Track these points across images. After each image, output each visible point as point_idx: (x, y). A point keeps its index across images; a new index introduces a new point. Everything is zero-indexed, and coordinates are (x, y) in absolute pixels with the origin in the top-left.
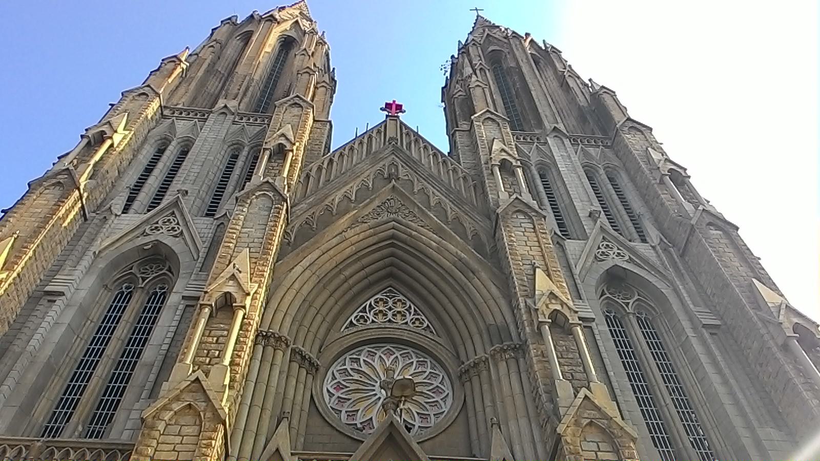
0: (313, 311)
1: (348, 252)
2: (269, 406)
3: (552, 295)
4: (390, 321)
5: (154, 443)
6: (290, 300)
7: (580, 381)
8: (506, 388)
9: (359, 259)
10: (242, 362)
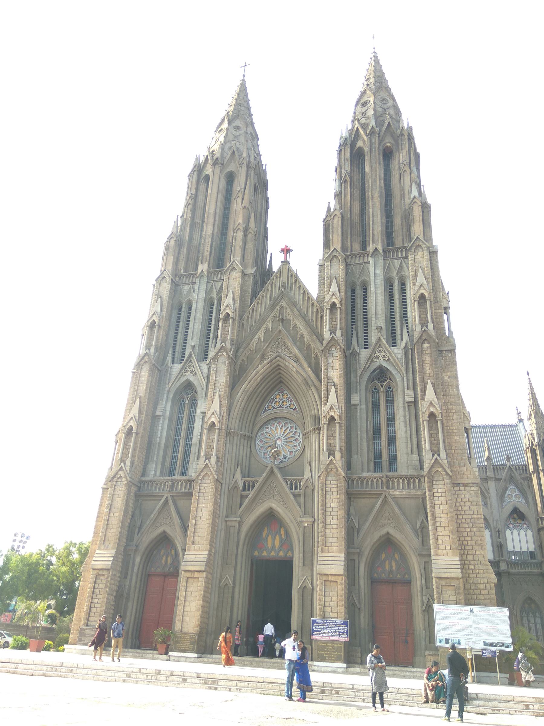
0: (248, 412)
1: (259, 379)
2: (233, 462)
7: (331, 452)
8: (314, 448)
9: (265, 380)
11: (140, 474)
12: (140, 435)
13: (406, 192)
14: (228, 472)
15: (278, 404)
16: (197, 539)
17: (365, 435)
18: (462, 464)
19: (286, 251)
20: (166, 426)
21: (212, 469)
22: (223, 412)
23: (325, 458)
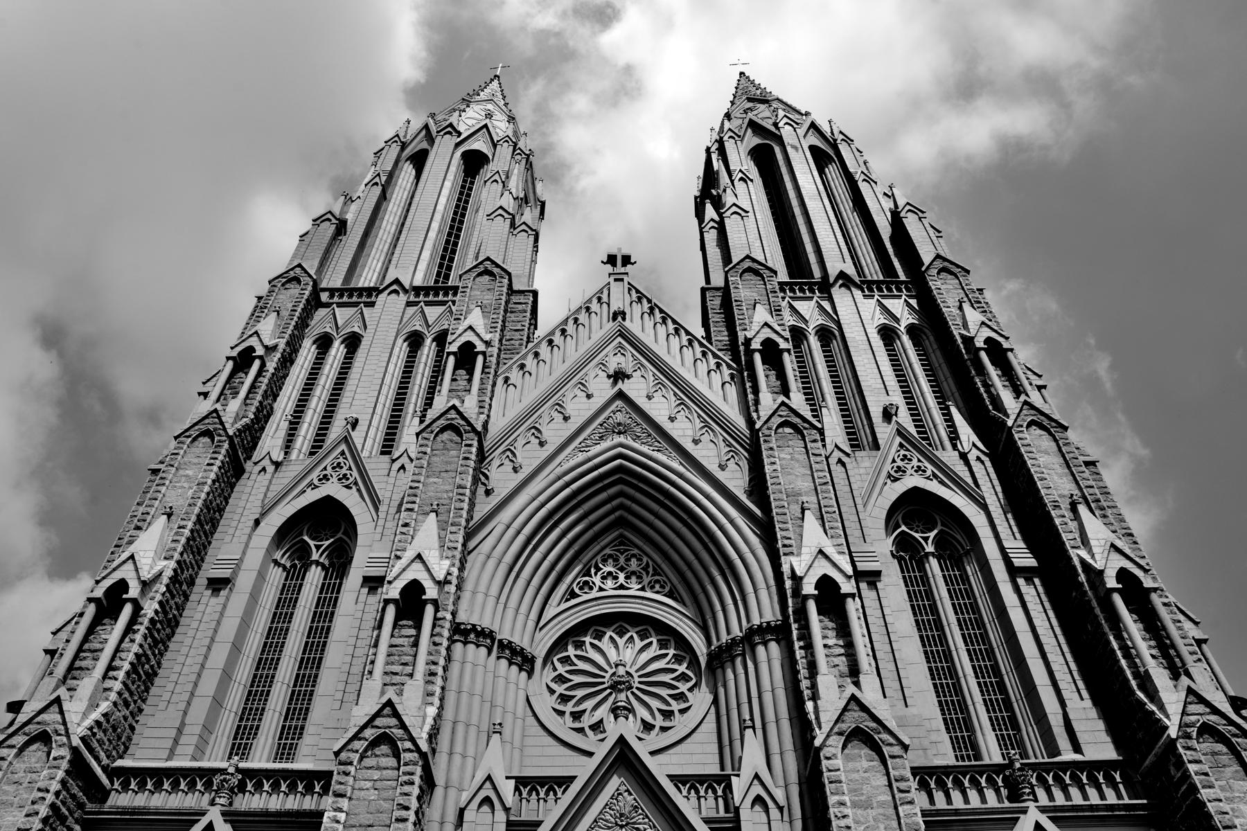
5: (351, 780)
22: (447, 563)
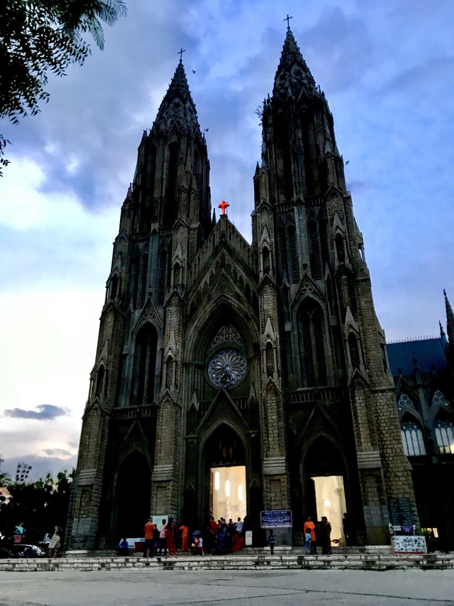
3: (268, 336)
4: (227, 339)
6: (190, 345)
7: (270, 373)
10: (178, 378)
11: (112, 405)
12: (110, 372)
13: (321, 149)
14: (186, 396)
15: (224, 336)
16: (162, 454)
17: (298, 357)
18: (379, 374)
19: (224, 206)
20: (132, 363)
21: (171, 396)
23: (265, 379)
